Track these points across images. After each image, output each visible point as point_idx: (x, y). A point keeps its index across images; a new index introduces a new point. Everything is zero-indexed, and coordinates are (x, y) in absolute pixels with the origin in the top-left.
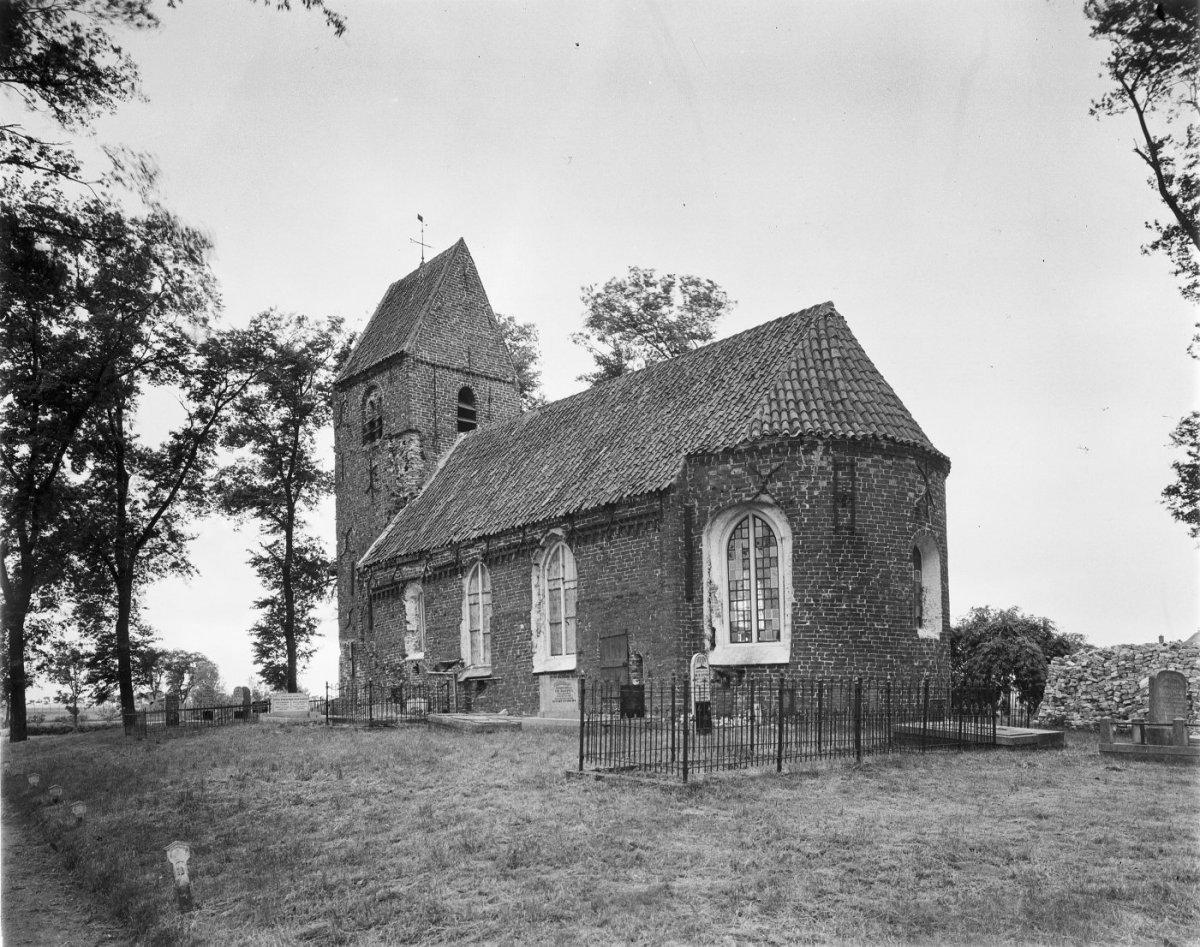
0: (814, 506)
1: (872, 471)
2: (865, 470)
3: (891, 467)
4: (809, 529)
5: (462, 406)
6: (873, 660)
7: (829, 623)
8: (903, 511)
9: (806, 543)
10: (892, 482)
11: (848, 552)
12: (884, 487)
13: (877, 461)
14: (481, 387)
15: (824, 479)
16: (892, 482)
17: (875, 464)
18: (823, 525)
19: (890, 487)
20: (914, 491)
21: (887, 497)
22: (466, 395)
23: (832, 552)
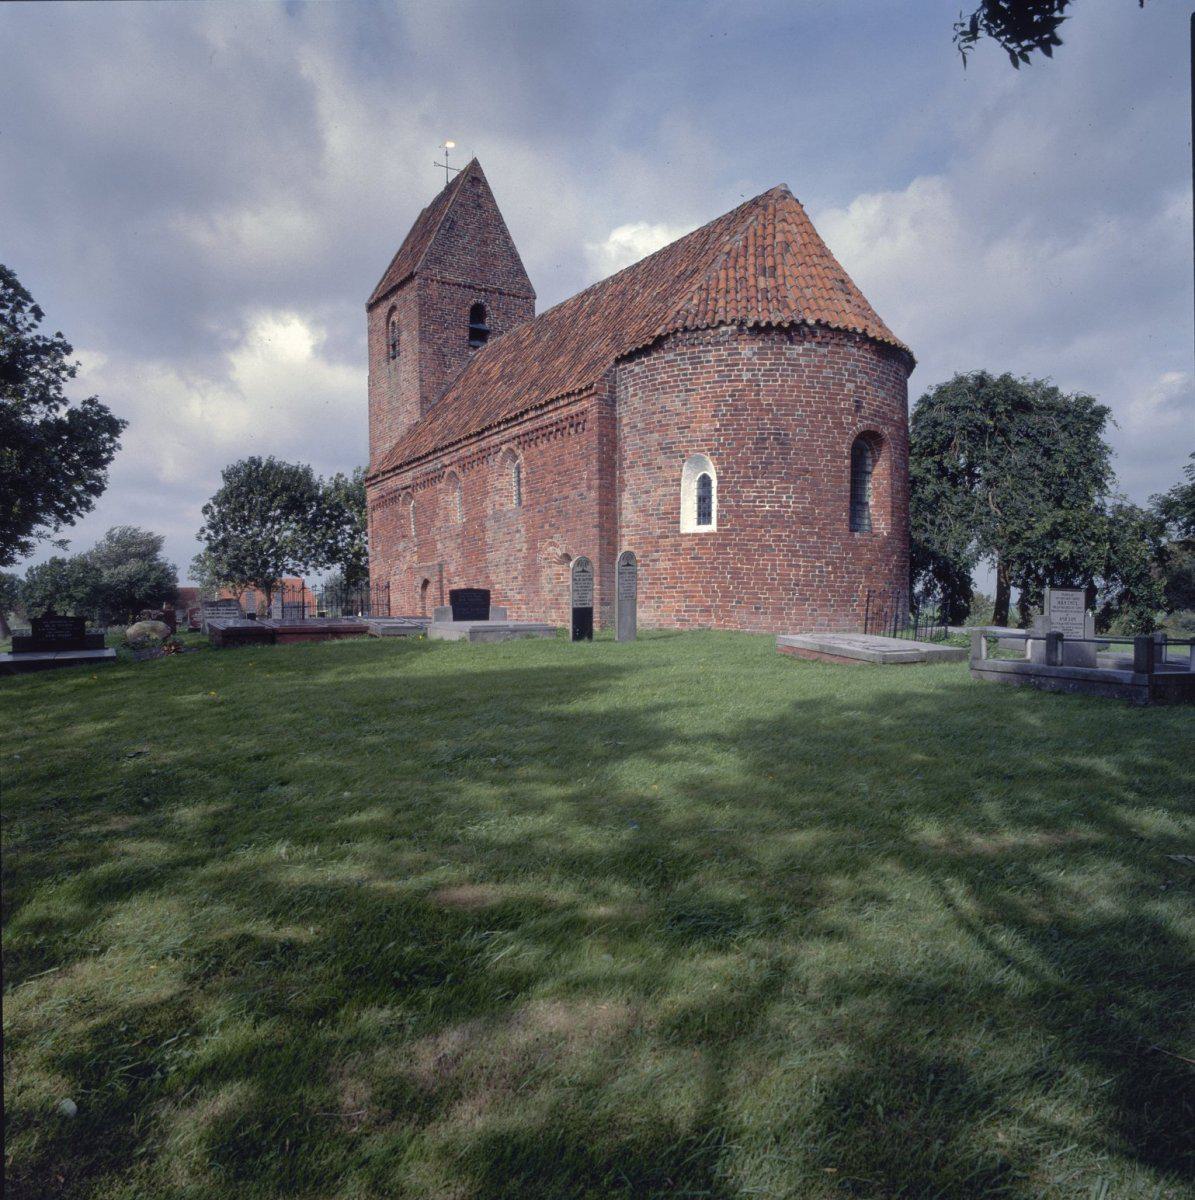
0: (736, 400)
1: (802, 361)
2: (794, 360)
3: (825, 356)
4: (732, 425)
5: (475, 326)
6: (799, 566)
7: (751, 526)
8: (839, 404)
9: (727, 440)
10: (827, 372)
11: (772, 449)
12: (818, 378)
13: (809, 350)
14: (494, 304)
15: (748, 370)
16: (827, 372)
17: (804, 354)
18: (746, 420)
19: (824, 377)
20: (855, 382)
21: (820, 388)
22: (478, 313)
23: (755, 449)
